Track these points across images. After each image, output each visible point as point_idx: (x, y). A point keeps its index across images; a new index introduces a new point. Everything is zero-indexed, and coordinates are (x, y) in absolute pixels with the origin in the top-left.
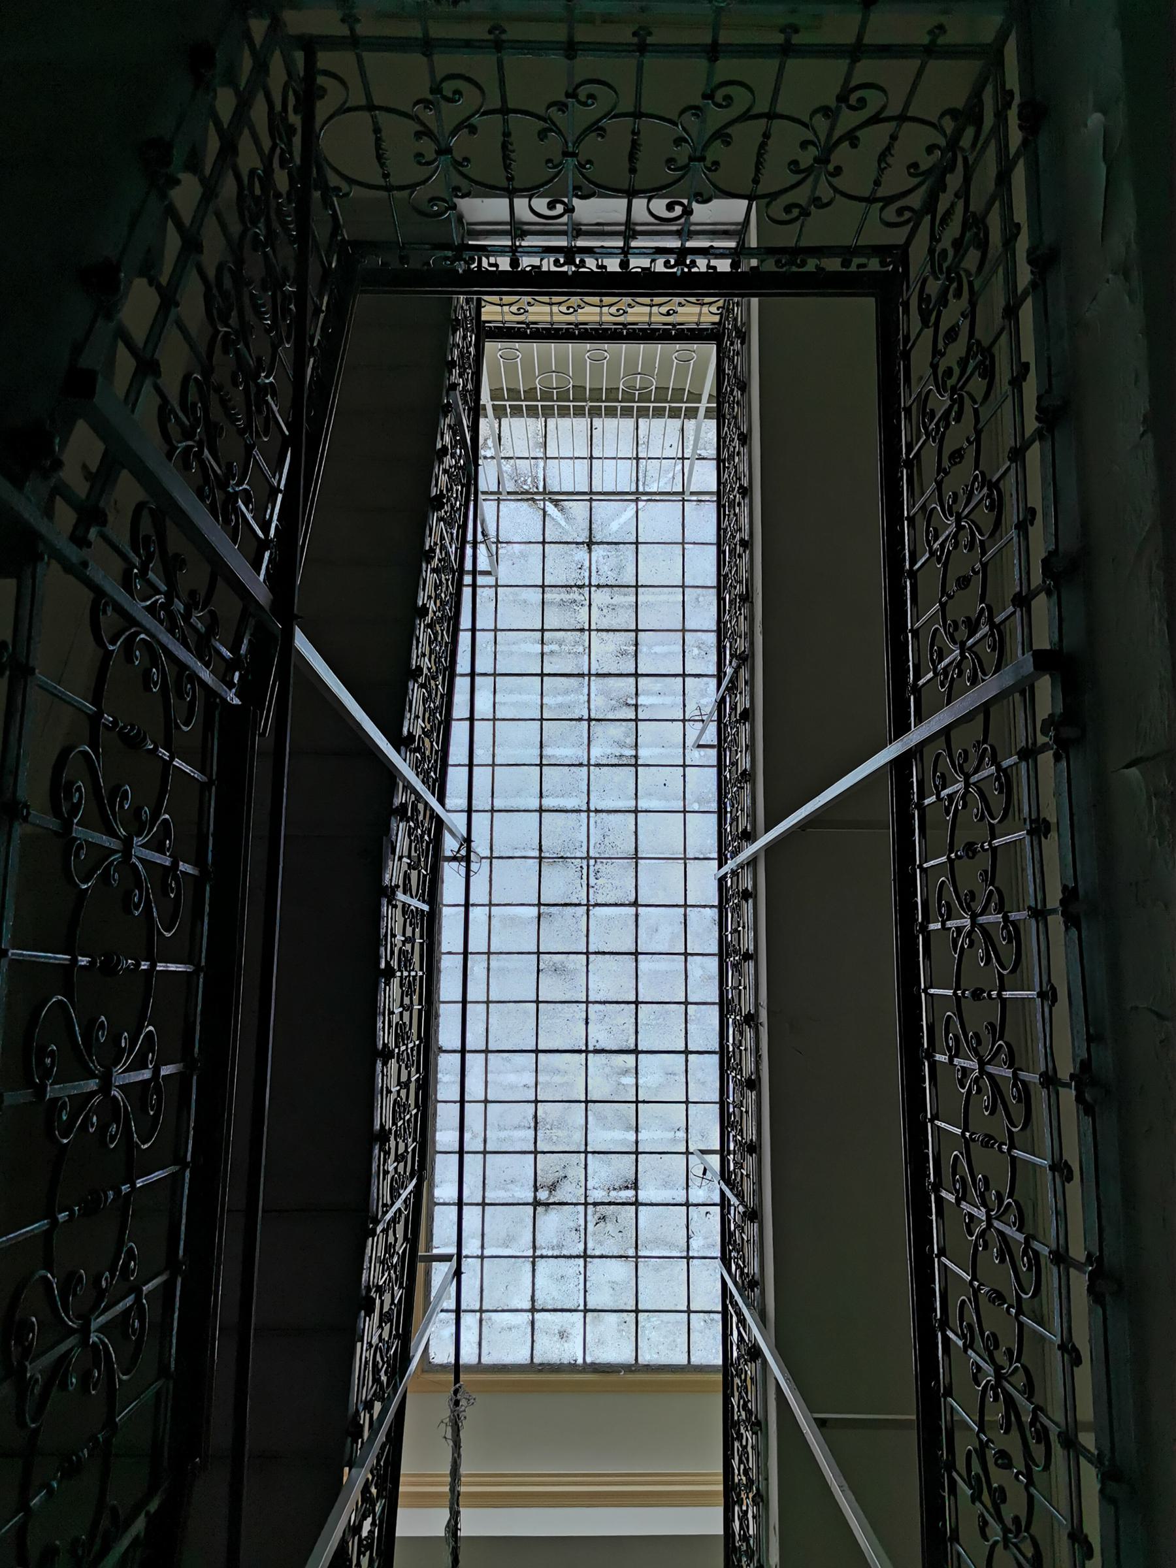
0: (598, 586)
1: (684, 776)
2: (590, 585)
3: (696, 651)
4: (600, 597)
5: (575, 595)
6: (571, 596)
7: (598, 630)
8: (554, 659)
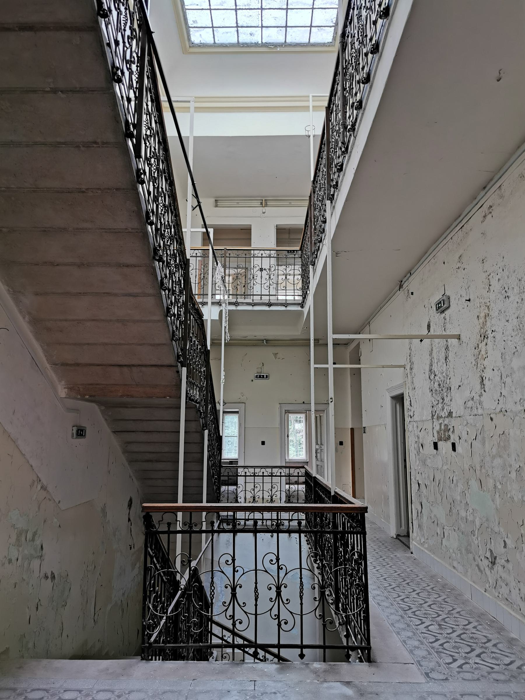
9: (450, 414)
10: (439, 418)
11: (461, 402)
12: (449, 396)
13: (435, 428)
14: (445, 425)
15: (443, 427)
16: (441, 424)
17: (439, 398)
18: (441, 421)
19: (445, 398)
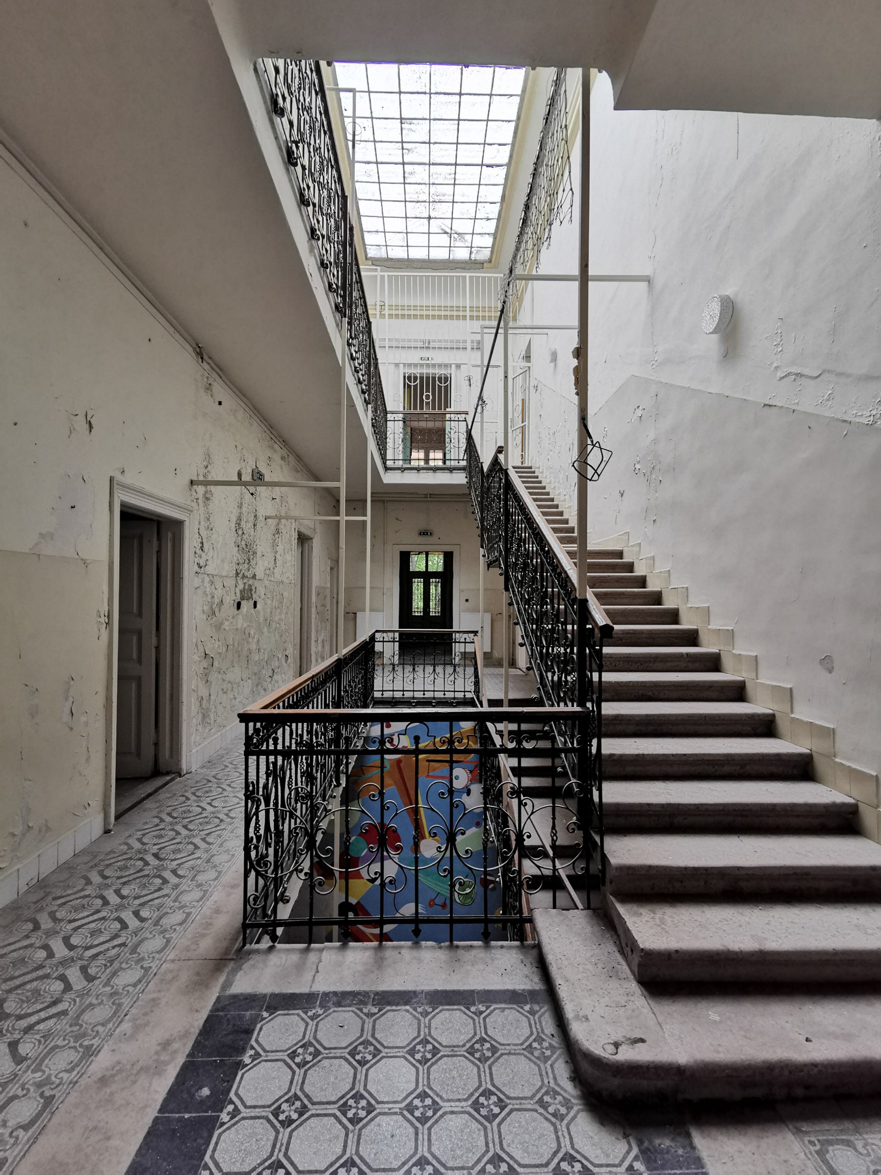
0: (425, 202)
1: (371, 112)
2: (429, 202)
3: (371, 173)
4: (426, 198)
5: (437, 199)
6: (438, 198)
7: (425, 184)
8: (449, 172)
9: (254, 577)
11: (262, 569)
15: (246, 587)
16: (245, 584)
17: (245, 558)
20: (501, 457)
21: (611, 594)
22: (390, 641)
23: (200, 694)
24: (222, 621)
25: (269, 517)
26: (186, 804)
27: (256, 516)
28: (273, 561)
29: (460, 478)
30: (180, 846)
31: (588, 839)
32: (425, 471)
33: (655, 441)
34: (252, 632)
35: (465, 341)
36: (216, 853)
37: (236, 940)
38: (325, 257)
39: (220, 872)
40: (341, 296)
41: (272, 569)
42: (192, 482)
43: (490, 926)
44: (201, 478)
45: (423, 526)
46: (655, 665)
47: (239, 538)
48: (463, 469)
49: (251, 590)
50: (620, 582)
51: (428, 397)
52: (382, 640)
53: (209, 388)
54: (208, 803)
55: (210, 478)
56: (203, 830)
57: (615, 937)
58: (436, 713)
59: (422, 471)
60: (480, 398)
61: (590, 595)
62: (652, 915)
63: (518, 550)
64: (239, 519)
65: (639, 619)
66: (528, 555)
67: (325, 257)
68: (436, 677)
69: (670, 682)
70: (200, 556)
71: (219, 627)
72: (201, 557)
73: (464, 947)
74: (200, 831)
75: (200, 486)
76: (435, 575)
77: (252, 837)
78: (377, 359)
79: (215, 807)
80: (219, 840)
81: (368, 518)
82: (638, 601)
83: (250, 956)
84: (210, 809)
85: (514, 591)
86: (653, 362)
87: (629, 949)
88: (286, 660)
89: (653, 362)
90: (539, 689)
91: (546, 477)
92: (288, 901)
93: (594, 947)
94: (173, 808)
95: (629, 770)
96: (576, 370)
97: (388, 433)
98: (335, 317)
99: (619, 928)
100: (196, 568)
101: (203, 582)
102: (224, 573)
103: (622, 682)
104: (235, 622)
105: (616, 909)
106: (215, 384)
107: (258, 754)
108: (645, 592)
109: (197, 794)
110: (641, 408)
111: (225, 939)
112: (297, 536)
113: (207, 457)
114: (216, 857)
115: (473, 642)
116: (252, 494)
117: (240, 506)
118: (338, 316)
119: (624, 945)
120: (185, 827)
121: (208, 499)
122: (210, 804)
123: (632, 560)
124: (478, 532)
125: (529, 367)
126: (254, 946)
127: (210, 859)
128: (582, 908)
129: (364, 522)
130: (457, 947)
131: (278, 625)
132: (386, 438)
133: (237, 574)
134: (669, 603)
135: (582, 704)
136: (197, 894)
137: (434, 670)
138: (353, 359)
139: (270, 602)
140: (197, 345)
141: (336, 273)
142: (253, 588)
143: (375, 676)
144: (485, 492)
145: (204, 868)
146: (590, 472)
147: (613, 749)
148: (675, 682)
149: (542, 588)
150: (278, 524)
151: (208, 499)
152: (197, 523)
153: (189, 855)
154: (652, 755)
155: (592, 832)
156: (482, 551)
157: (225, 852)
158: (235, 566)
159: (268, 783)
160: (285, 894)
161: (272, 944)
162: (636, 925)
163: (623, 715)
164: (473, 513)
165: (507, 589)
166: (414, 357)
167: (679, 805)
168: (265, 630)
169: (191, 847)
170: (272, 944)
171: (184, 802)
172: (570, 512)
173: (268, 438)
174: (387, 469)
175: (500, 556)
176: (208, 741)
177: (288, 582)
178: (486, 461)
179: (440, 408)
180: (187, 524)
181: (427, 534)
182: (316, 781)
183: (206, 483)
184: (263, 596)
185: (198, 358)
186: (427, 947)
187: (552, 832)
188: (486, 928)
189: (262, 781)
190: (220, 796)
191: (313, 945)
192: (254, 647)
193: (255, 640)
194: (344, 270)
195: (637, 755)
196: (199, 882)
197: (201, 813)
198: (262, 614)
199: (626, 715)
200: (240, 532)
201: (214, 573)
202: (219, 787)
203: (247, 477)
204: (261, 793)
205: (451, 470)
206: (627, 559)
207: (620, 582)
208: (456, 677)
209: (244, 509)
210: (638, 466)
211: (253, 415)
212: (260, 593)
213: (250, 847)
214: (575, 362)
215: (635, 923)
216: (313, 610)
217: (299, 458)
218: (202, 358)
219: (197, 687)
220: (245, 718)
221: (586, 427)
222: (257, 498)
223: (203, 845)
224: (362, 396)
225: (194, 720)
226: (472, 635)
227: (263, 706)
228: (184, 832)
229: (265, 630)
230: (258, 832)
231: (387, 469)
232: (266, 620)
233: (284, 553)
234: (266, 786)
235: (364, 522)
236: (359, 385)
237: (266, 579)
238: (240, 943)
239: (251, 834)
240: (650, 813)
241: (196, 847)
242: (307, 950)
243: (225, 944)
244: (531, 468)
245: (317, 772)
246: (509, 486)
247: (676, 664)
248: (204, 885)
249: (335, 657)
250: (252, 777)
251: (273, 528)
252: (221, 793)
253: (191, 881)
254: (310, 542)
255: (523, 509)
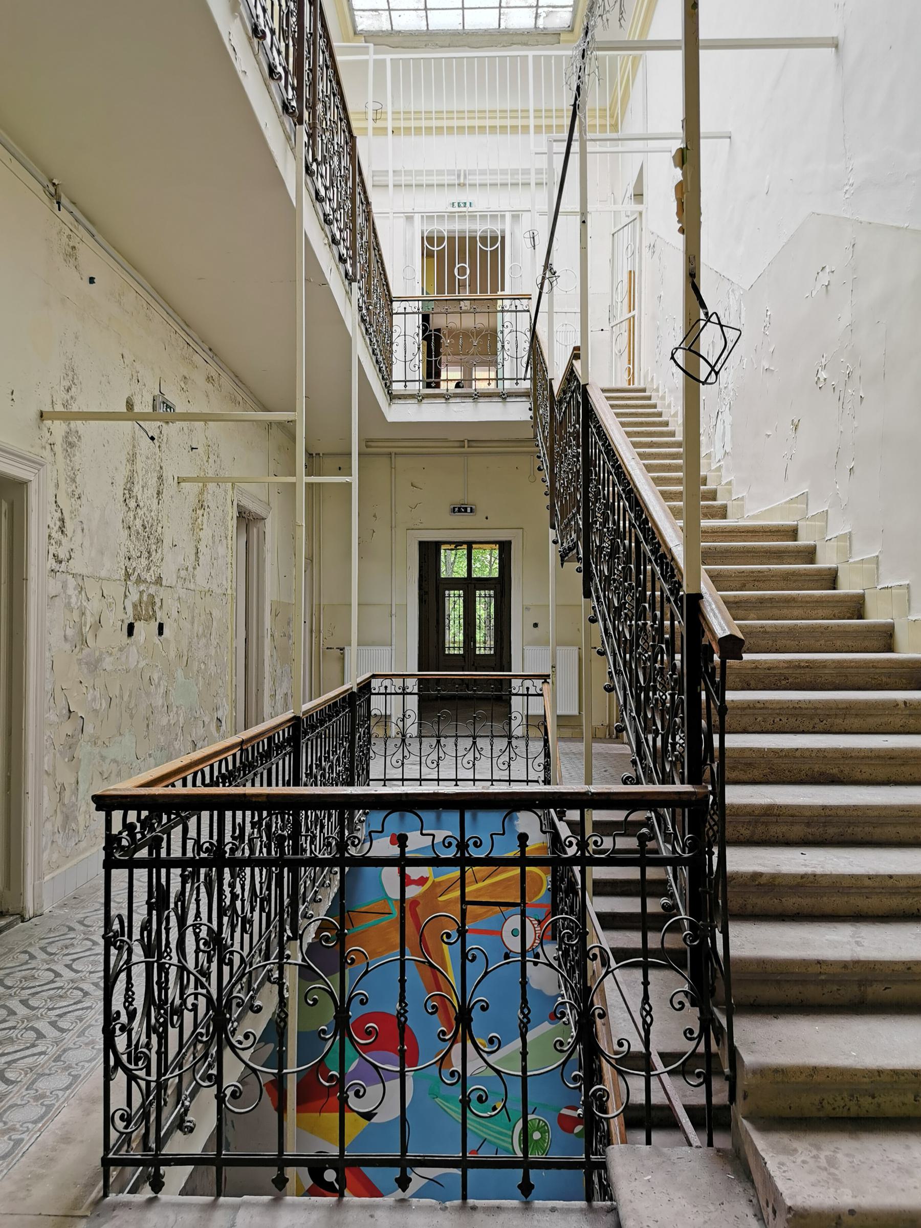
9: (159, 581)
10: (139, 580)
12: (159, 551)
13: (130, 597)
14: (149, 595)
15: (145, 598)
16: (141, 593)
17: (142, 548)
18: (142, 587)
19: (154, 553)
20: (577, 364)
21: (771, 599)
22: (396, 694)
23: (59, 780)
24: (101, 654)
25: (185, 480)
26: (29, 966)
27: (160, 478)
28: (193, 557)
29: (519, 411)
30: (13, 1034)
31: (707, 1022)
32: (458, 400)
33: (852, 328)
34: (155, 677)
35: (526, 172)
36: (71, 1046)
37: (94, 1185)
38: (261, 20)
39: (76, 1077)
40: (293, 88)
41: (191, 569)
42: (42, 415)
43: (532, 1173)
44: (59, 408)
45: (458, 499)
46: (847, 721)
47: (131, 514)
48: (526, 394)
49: (153, 604)
50: (789, 580)
51: (462, 271)
52: (382, 690)
53: (72, 253)
54: (66, 966)
55: (75, 408)
56: (53, 1009)
57: (751, 1192)
58: (434, 794)
59: (452, 400)
60: (547, 266)
61: (706, 588)
62: (815, 1152)
63: (604, 524)
64: (131, 480)
65: (822, 642)
66: (619, 534)
67: (261, 20)
68: (477, 755)
69: (871, 750)
70: (59, 543)
71: (94, 665)
72: (61, 544)
73: (488, 1210)
74: (49, 1009)
75: (57, 422)
76: (484, 583)
77: (118, 1013)
78: (368, 204)
79: (77, 972)
80: (79, 1025)
81: (354, 479)
82: (820, 612)
83: (115, 1213)
84: (68, 974)
85: (598, 598)
86: (847, 187)
87: (770, 1210)
88: (219, 727)
89: (847, 187)
90: (634, 762)
91: (669, 406)
92: (191, 1130)
93: (712, 1208)
94: (8, 971)
95: (791, 903)
96: (680, 188)
97: (395, 335)
98: (282, 124)
99: (757, 1177)
100: (52, 563)
101: (64, 586)
102: (103, 574)
103: (782, 750)
104: (123, 659)
105: (752, 1141)
106: (81, 247)
107: (132, 865)
108: (833, 596)
109: (49, 950)
110: (827, 270)
111: (75, 1184)
112: (236, 514)
113: (70, 374)
114: (70, 1053)
115: (542, 695)
116: (152, 438)
117: (132, 459)
118: (288, 121)
119: (763, 1204)
120: (24, 1002)
121: (71, 445)
122: (69, 966)
123: (812, 543)
124: (547, 500)
125: (641, 213)
126: (125, 1197)
127: (60, 1056)
128: (699, 1144)
129: (349, 485)
130: (474, 1208)
131: (203, 666)
132: (392, 343)
133: (128, 576)
134: (876, 616)
135: (694, 779)
136: (36, 1110)
137: (474, 743)
138: (318, 198)
139: (189, 626)
140: (51, 181)
141: (283, 49)
142: (157, 600)
143: (372, 754)
144: (557, 428)
145: (50, 1069)
146: (704, 370)
147: (760, 864)
148: (880, 750)
149: (638, 585)
150: (201, 493)
151: (71, 445)
152: (51, 485)
153: (28, 1048)
154: (830, 876)
155: (715, 1010)
156: (552, 534)
157: (87, 1044)
158: (123, 562)
159: (150, 921)
160: (187, 1118)
161: (152, 1195)
162: (785, 1168)
163: (780, 807)
164: (539, 469)
165: (587, 594)
166: (440, 202)
167: (875, 963)
168: (179, 674)
169: (32, 1035)
170: (152, 1195)
171: (26, 963)
172: (709, 464)
173: (182, 343)
174: (392, 397)
175: (578, 538)
176: (75, 861)
177: (219, 591)
178: (557, 374)
179: (484, 291)
180: (33, 488)
181: (466, 511)
182: (251, 925)
183: (68, 416)
184: (174, 614)
185: (52, 203)
186: (419, 1208)
187: (643, 1008)
188: (526, 1176)
189: (139, 916)
190: (88, 953)
191: (222, 1199)
192: (159, 702)
193: (162, 690)
194: (299, 43)
195: (803, 876)
196: (40, 1091)
197: (53, 982)
198: (173, 646)
199: (787, 807)
200: (132, 504)
201: (84, 572)
202: (87, 939)
203: (143, 406)
204: (136, 935)
205: (504, 396)
206: (803, 541)
207: (789, 580)
208: (513, 755)
209: (139, 465)
210: (823, 375)
211: (153, 303)
212: (168, 612)
213: (114, 1029)
214: (677, 174)
215: (783, 1164)
216: (267, 641)
217: (237, 378)
218: (58, 203)
219: (55, 768)
220: (105, 803)
221: (696, 289)
222: (163, 446)
223: (50, 1032)
224: (341, 265)
225: (48, 826)
226: (538, 682)
227: (138, 784)
228: (22, 1011)
229: (179, 674)
230: (131, 1004)
231: (392, 397)
232: (180, 657)
233: (214, 542)
234: (146, 926)
235: (349, 485)
236: (334, 247)
237: (180, 585)
238: (99, 1192)
239: (118, 1004)
240: (823, 977)
241: (40, 1035)
242: (213, 1206)
243: (74, 1192)
244: (644, 390)
245: (252, 910)
246: (589, 414)
247: (885, 720)
248: (48, 1097)
249: (289, 715)
250: (119, 907)
251: (193, 500)
252: (90, 949)
253: (27, 1089)
254: (260, 524)
255: (611, 452)
